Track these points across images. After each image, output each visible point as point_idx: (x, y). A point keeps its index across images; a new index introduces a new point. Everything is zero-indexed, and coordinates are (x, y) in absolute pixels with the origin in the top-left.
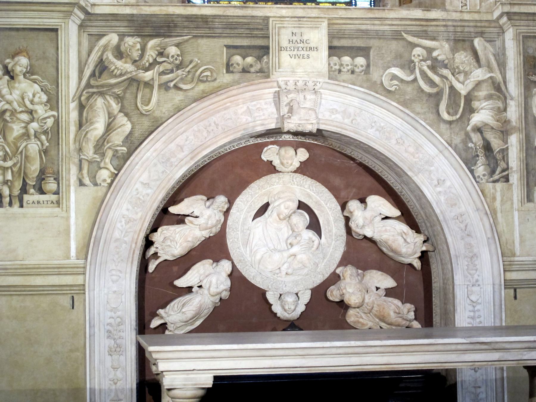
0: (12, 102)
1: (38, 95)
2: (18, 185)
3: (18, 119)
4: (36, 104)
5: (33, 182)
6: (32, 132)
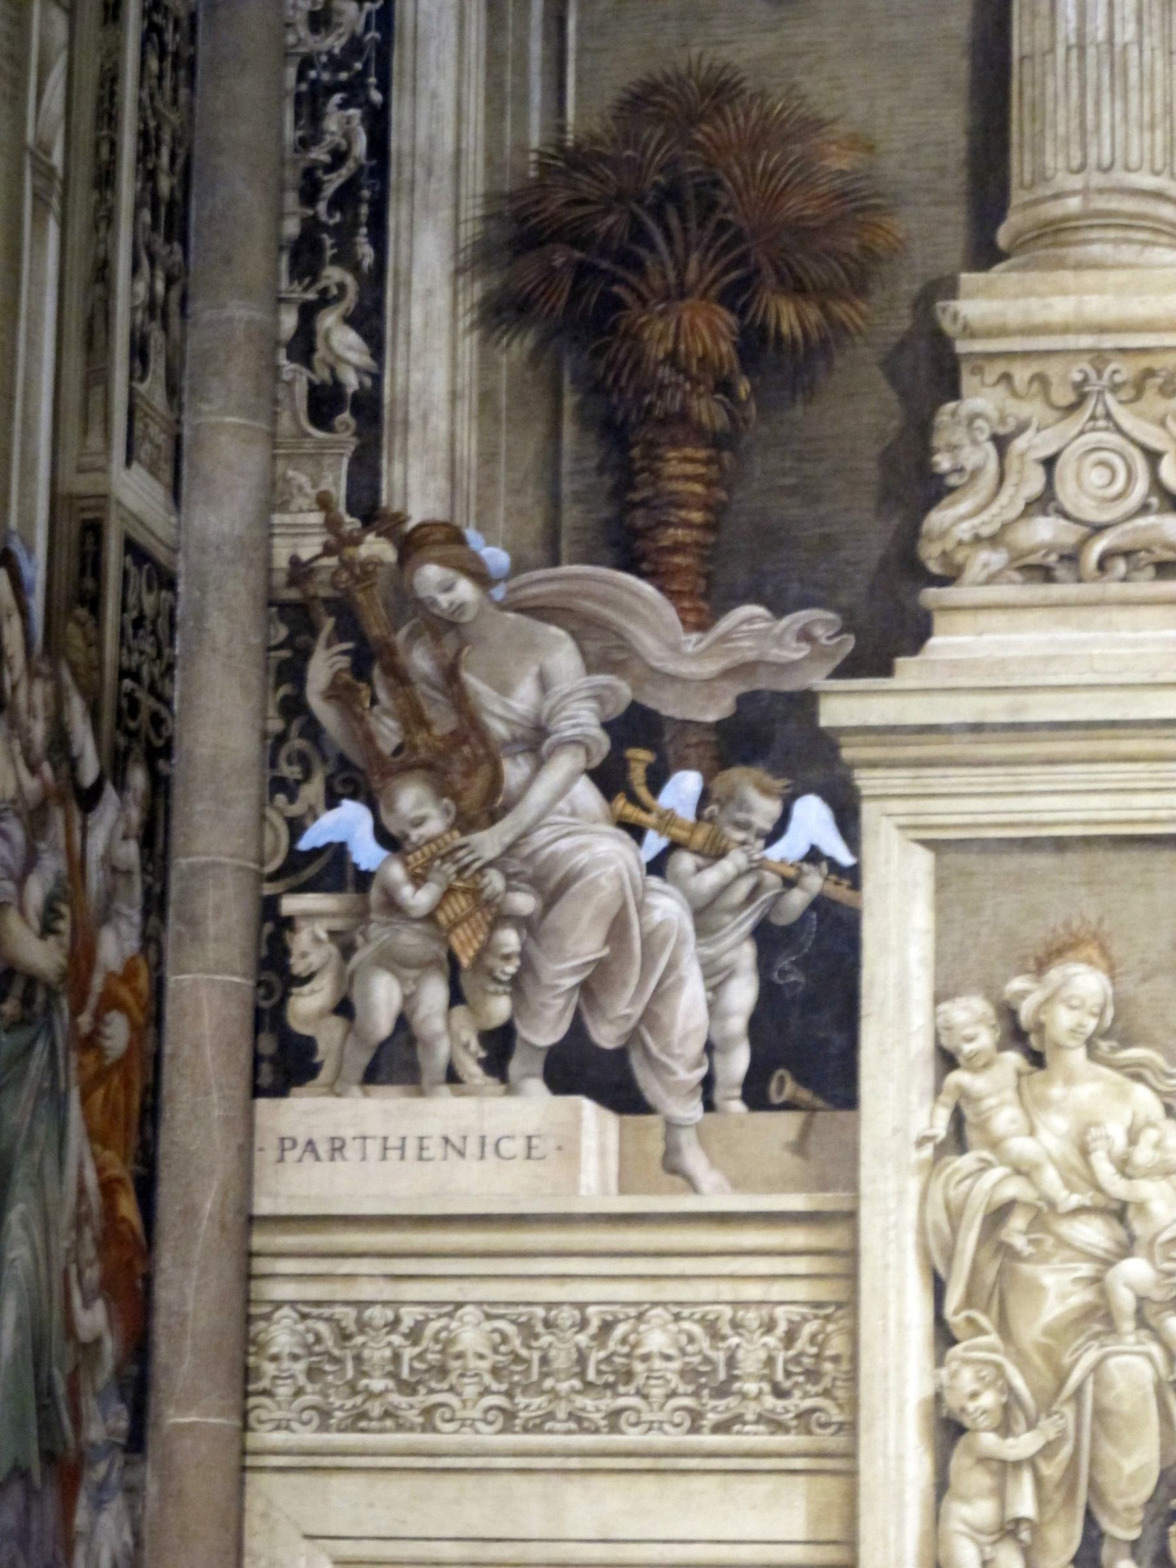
0: (1037, 1166)
1: (1150, 1135)
3: (1063, 1243)
4: (1144, 1176)
5: (1130, 1526)
6: (1125, 1300)
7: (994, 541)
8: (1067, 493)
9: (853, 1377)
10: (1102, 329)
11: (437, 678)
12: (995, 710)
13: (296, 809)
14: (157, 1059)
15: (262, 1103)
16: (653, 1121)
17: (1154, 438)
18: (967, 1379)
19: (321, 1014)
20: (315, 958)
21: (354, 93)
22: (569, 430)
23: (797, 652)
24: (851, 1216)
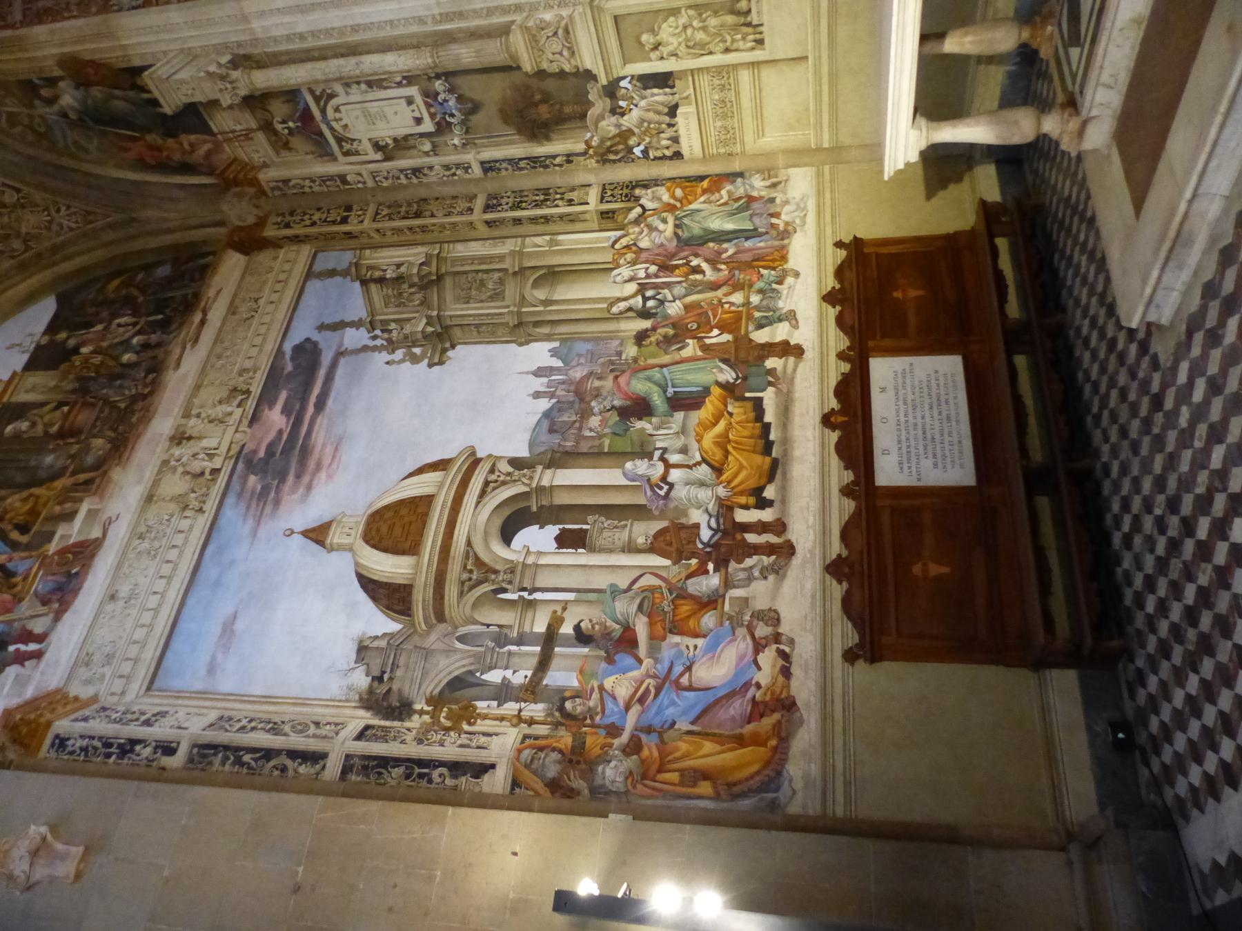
2: (745, 29)
6: (701, 24)
7: (569, 61)
8: (558, 50)
9: (720, 66)
10: (527, 48)
12: (599, 58)
16: (680, 102)
17: (545, 38)
18: (718, 48)
21: (517, 163)
23: (595, 90)
24: (692, 70)
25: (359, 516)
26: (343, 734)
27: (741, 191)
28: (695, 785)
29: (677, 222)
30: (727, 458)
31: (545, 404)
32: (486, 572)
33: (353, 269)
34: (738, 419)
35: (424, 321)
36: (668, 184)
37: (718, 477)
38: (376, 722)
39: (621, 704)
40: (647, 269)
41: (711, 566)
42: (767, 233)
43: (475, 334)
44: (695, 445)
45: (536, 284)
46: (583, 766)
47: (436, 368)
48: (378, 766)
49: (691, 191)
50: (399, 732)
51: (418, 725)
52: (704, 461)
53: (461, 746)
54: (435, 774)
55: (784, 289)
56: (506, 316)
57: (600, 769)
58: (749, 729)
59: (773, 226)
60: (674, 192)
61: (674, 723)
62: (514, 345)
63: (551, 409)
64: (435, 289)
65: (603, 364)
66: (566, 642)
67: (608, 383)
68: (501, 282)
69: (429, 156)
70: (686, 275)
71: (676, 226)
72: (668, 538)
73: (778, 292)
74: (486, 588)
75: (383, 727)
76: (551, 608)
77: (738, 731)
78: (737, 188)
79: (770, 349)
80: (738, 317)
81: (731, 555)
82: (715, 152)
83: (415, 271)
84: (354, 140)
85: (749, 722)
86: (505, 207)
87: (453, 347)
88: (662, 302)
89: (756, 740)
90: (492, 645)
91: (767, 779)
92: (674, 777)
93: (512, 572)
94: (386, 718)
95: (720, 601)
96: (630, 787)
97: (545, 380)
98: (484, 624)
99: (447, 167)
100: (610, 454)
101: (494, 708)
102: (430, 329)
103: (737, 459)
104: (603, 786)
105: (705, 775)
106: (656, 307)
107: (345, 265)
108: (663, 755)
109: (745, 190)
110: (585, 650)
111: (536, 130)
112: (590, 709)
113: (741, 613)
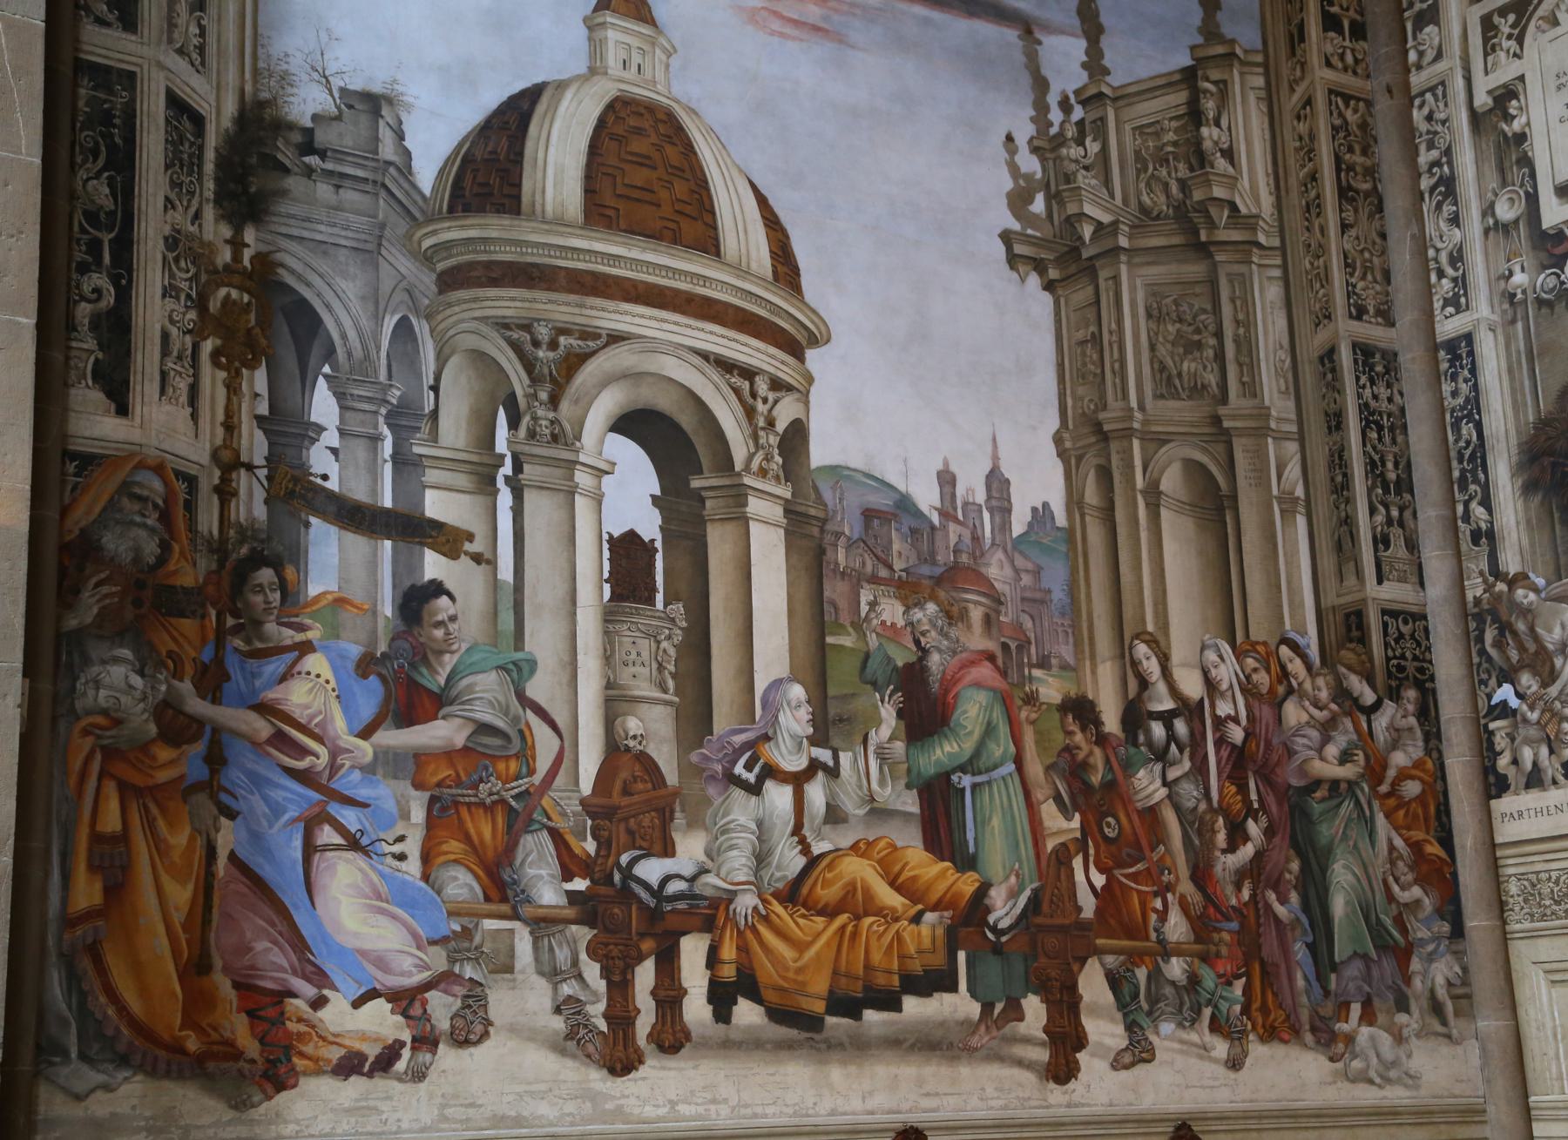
11: (1527, 632)
13: (1488, 690)
14: (1445, 793)
15: (1493, 803)
19: (1508, 765)
20: (1503, 745)
21: (1469, 417)
22: (1558, 527)
25: (669, 86)
26: (181, 65)
27: (1422, 933)
28: (92, 868)
29: (1343, 786)
30: (820, 913)
31: (927, 497)
32: (553, 380)
33: (1220, 50)
34: (906, 936)
35: (1106, 218)
36: (1430, 765)
37: (776, 895)
38: (212, 140)
39: (271, 695)
40: (1236, 720)
41: (580, 884)
42: (1327, 993)
43: (1080, 335)
44: (846, 842)
45: (1194, 469)
46: (129, 614)
47: (1000, 249)
48: (112, 148)
49: (1415, 816)
50: (192, 194)
51: (208, 235)
52: (813, 862)
53: (165, 336)
54: (99, 280)
55: (1201, 1033)
56: (1120, 404)
57: (126, 653)
58: (224, 986)
59: (1345, 1006)
60: (1412, 778)
61: (232, 815)
62: (1054, 423)
63: (918, 514)
64: (1176, 240)
65: (1019, 626)
66: (405, 566)
67: (977, 640)
68: (1198, 390)
69: (1484, 215)
70: (1224, 810)
71: (1335, 784)
72: (640, 786)
73: (1193, 1021)
74: (519, 382)
75: (200, 157)
76: (478, 527)
77: (218, 963)
78: (1427, 922)
79: (1064, 1006)
80: (1135, 930)
81: (606, 930)
82: (1511, 871)
83: (1218, 192)
84: (1520, 41)
85: (237, 985)
86: (1368, 392)
87: (1049, 286)
88: (1161, 755)
89: (198, 1002)
90: (394, 396)
91: (110, 1032)
92: (111, 821)
93: (555, 438)
94: (221, 163)
95: (505, 908)
96: (83, 723)
97: (980, 497)
98: (438, 378)
99: (1457, 258)
100: (822, 649)
101: (252, 407)
102: (1087, 231)
103: (819, 934)
104: (87, 661)
105: (117, 888)
106: (1150, 744)
107: (1228, 30)
108: (155, 791)
109: (1422, 942)
110: (387, 609)
111: (1547, 461)
112: (258, 624)
113: (477, 957)
